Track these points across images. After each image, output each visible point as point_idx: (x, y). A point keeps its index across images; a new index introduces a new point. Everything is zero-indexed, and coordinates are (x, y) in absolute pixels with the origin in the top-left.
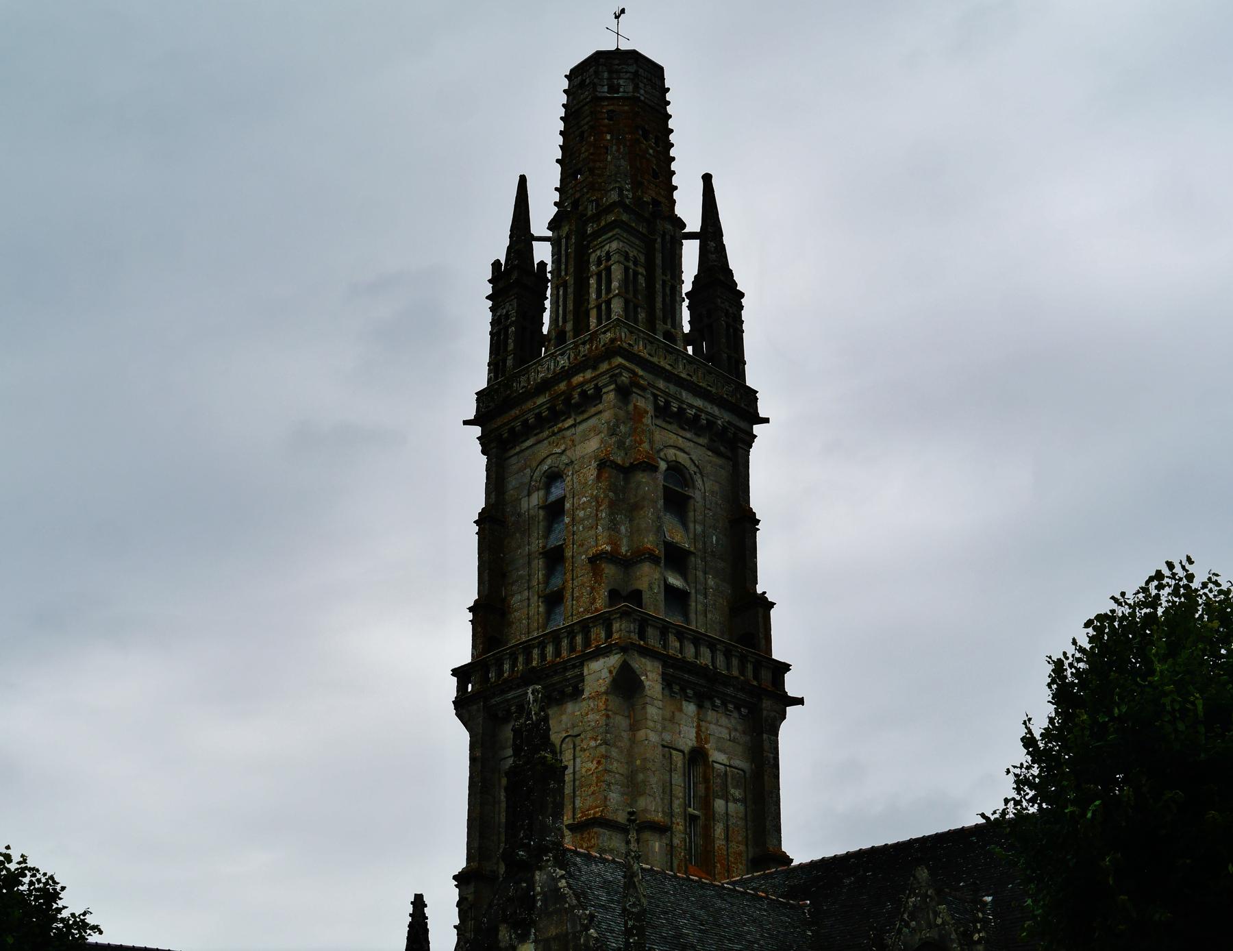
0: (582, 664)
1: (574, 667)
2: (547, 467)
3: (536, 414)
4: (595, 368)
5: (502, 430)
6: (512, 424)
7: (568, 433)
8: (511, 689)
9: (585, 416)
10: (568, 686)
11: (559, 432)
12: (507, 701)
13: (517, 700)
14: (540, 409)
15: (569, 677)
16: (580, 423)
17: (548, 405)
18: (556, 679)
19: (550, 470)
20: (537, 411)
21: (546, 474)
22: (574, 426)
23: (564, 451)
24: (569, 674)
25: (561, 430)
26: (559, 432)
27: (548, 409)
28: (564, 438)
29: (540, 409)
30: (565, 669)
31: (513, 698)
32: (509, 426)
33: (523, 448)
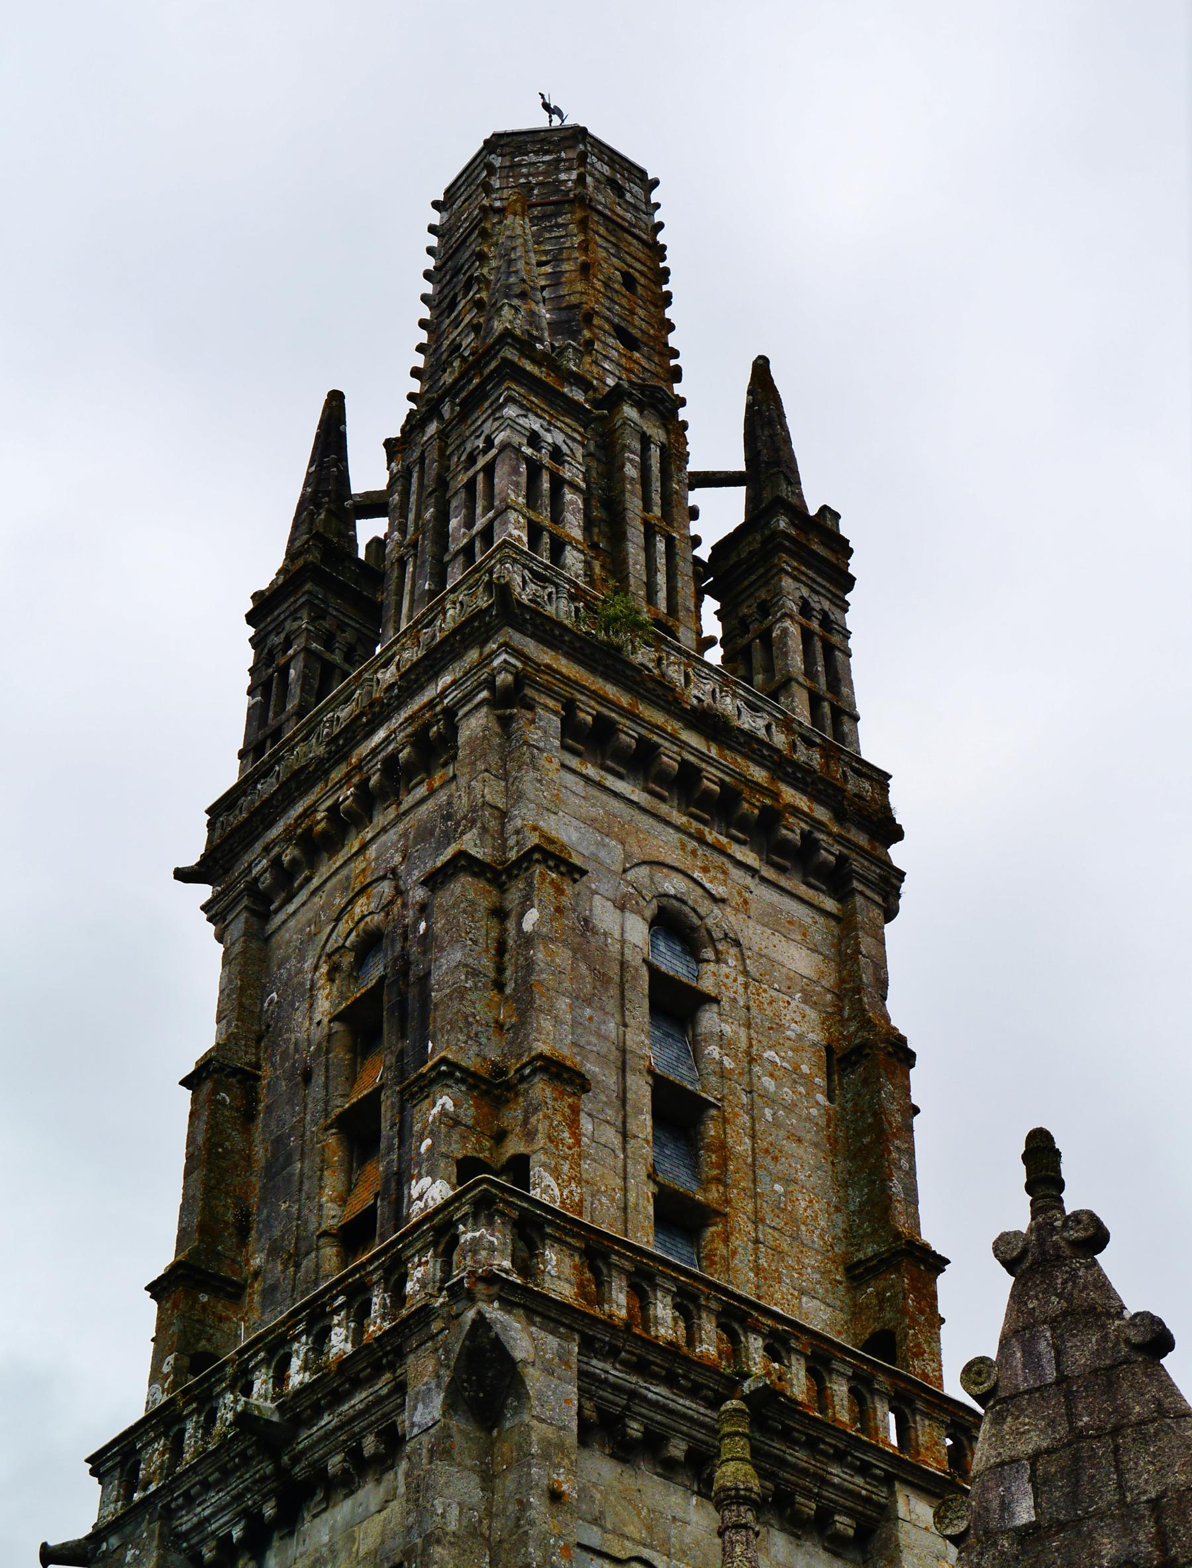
0: (888, 1481)
1: (864, 1470)
2: (672, 892)
3: (683, 759)
4: (840, 816)
5: (583, 698)
6: (613, 715)
7: (736, 873)
8: (670, 1381)
9: (783, 882)
10: (809, 1495)
11: (713, 847)
12: (633, 1395)
13: (659, 1417)
14: (704, 765)
15: (836, 1480)
16: (764, 880)
17: (727, 779)
18: (799, 1456)
19: (674, 902)
20: (692, 758)
21: (664, 901)
22: (753, 872)
23: (723, 901)
24: (837, 1473)
25: (722, 852)
26: (713, 847)
27: (722, 783)
28: (724, 872)
29: (704, 765)
30: (839, 1457)
31: (654, 1405)
32: (606, 712)
33: (608, 784)
